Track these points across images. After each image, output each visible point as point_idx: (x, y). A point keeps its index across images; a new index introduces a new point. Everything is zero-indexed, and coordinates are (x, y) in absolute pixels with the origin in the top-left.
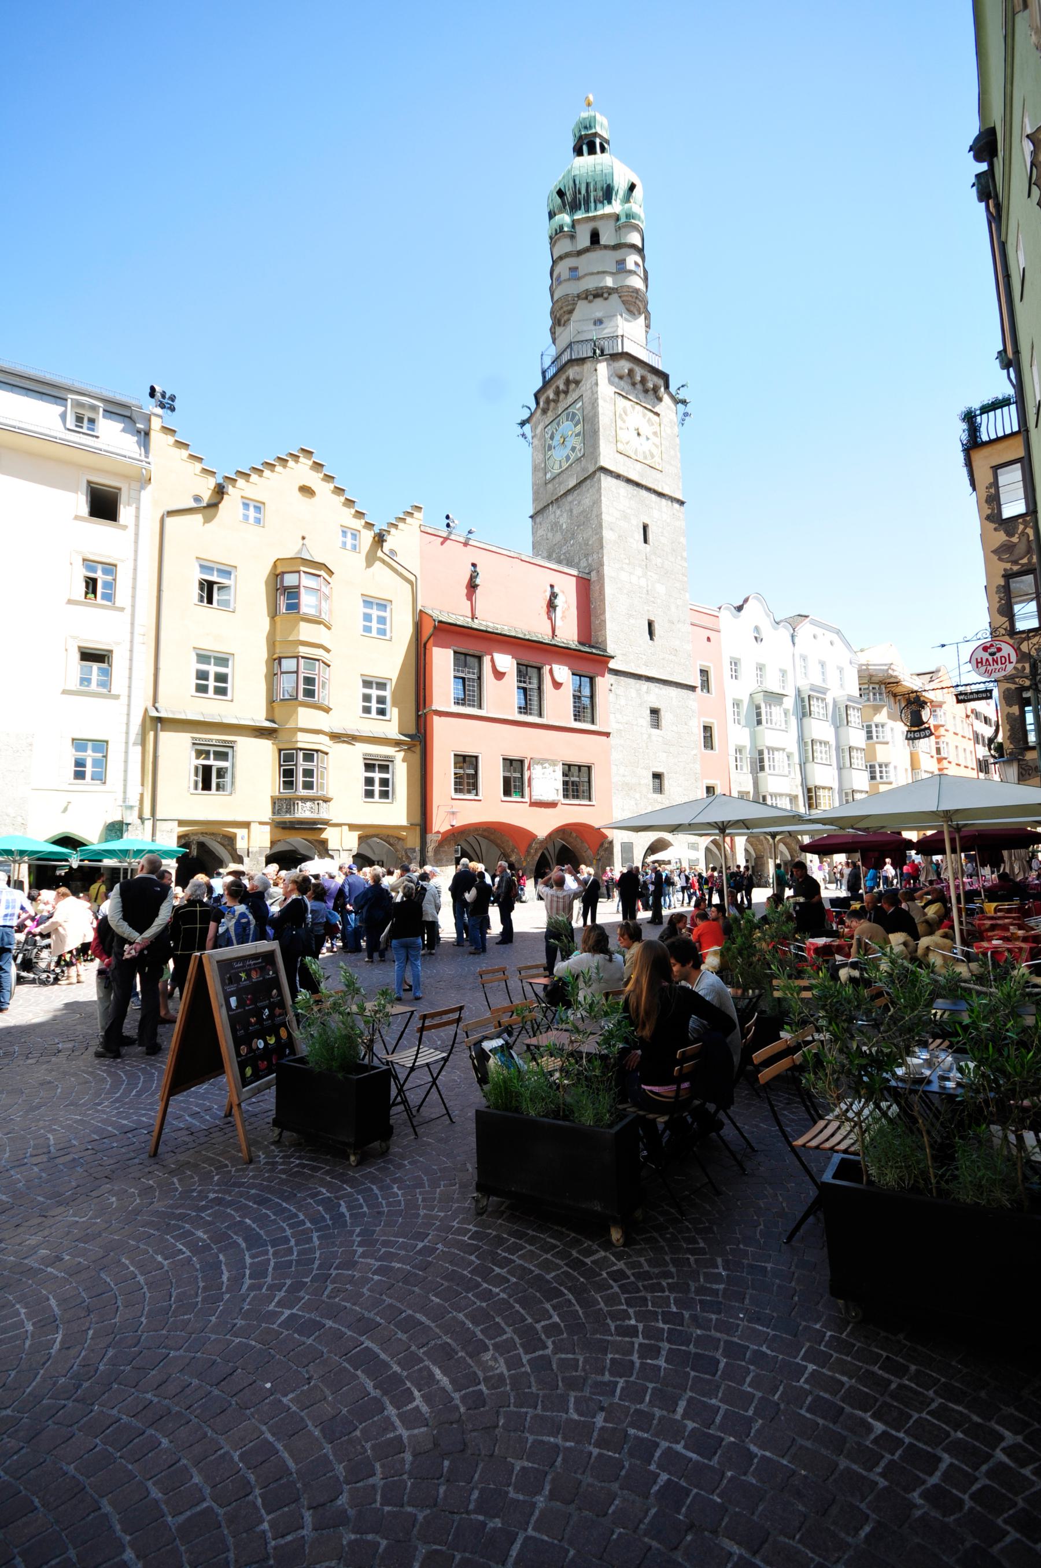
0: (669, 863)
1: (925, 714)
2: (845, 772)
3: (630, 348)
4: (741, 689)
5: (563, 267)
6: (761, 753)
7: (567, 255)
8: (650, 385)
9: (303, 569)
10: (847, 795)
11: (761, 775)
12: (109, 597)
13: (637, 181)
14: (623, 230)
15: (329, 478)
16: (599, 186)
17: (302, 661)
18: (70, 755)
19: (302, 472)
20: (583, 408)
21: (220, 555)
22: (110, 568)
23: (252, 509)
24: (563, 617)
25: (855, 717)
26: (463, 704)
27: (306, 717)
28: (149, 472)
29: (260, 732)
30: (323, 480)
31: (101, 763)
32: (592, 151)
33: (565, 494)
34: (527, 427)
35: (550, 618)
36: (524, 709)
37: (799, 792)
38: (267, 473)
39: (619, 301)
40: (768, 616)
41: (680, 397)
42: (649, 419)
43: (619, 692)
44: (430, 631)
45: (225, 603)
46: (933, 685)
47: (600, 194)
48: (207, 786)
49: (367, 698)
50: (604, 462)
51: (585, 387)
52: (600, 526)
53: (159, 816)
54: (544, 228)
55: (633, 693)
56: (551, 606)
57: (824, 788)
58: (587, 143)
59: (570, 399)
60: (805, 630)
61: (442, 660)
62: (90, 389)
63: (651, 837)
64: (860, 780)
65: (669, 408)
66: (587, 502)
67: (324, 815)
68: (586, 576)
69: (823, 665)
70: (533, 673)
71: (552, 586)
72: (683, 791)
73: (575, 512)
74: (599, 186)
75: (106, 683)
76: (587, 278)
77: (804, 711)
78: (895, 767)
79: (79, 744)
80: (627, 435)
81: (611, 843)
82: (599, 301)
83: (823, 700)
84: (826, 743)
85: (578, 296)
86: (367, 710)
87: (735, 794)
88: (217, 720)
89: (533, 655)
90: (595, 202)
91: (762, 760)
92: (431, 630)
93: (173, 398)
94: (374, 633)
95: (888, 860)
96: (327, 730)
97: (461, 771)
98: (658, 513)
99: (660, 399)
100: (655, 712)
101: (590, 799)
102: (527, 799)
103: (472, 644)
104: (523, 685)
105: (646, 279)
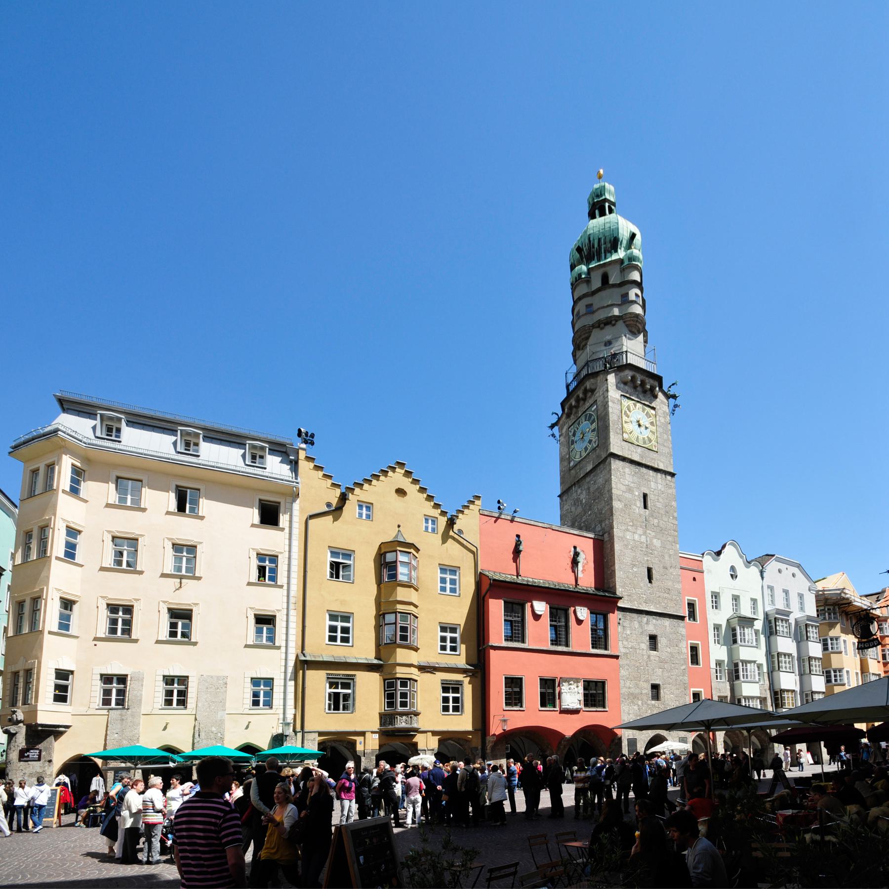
0: (664, 753)
1: (874, 628)
2: (805, 677)
3: (632, 360)
4: (721, 616)
5: (581, 306)
6: (736, 665)
7: (585, 296)
8: (648, 387)
9: (399, 548)
10: (807, 694)
11: (736, 682)
12: (273, 578)
13: (636, 231)
14: (626, 271)
15: (416, 482)
16: (608, 240)
17: (399, 615)
18: (249, 689)
19: (398, 478)
21: (342, 543)
22: (274, 559)
23: (364, 509)
24: (583, 571)
25: (813, 633)
26: (511, 640)
27: (402, 656)
28: (298, 489)
29: (370, 667)
30: (412, 483)
31: (269, 694)
32: (602, 214)
34: (556, 428)
35: (573, 571)
36: (555, 642)
37: (768, 695)
38: (374, 482)
39: (623, 325)
40: (741, 557)
41: (671, 393)
43: (625, 624)
44: (487, 588)
45: (347, 578)
46: (882, 603)
48: (337, 708)
49: (443, 639)
50: (614, 449)
51: (598, 394)
52: (611, 498)
53: (306, 729)
54: (567, 277)
56: (575, 563)
57: (788, 691)
58: (598, 207)
59: (587, 405)
60: (772, 566)
61: (496, 608)
62: (262, 436)
63: (651, 733)
64: (818, 683)
65: (662, 402)
66: (601, 481)
67: (415, 725)
68: (600, 538)
69: (786, 592)
70: (561, 614)
71: (575, 548)
72: (674, 697)
73: (591, 489)
75: (271, 638)
77: (770, 630)
78: (848, 672)
79: (255, 681)
80: (630, 427)
81: (620, 739)
82: (608, 328)
83: (787, 621)
84: (789, 655)
86: (443, 648)
87: (715, 698)
88: (343, 660)
89: (561, 600)
91: (737, 671)
92: (488, 587)
93: (313, 436)
94: (448, 592)
95: (843, 748)
96: (416, 664)
97: (510, 690)
98: (656, 484)
99: (656, 397)
100: (653, 638)
101: (604, 707)
102: (557, 709)
103: (516, 595)
104: (554, 623)
105: (644, 307)
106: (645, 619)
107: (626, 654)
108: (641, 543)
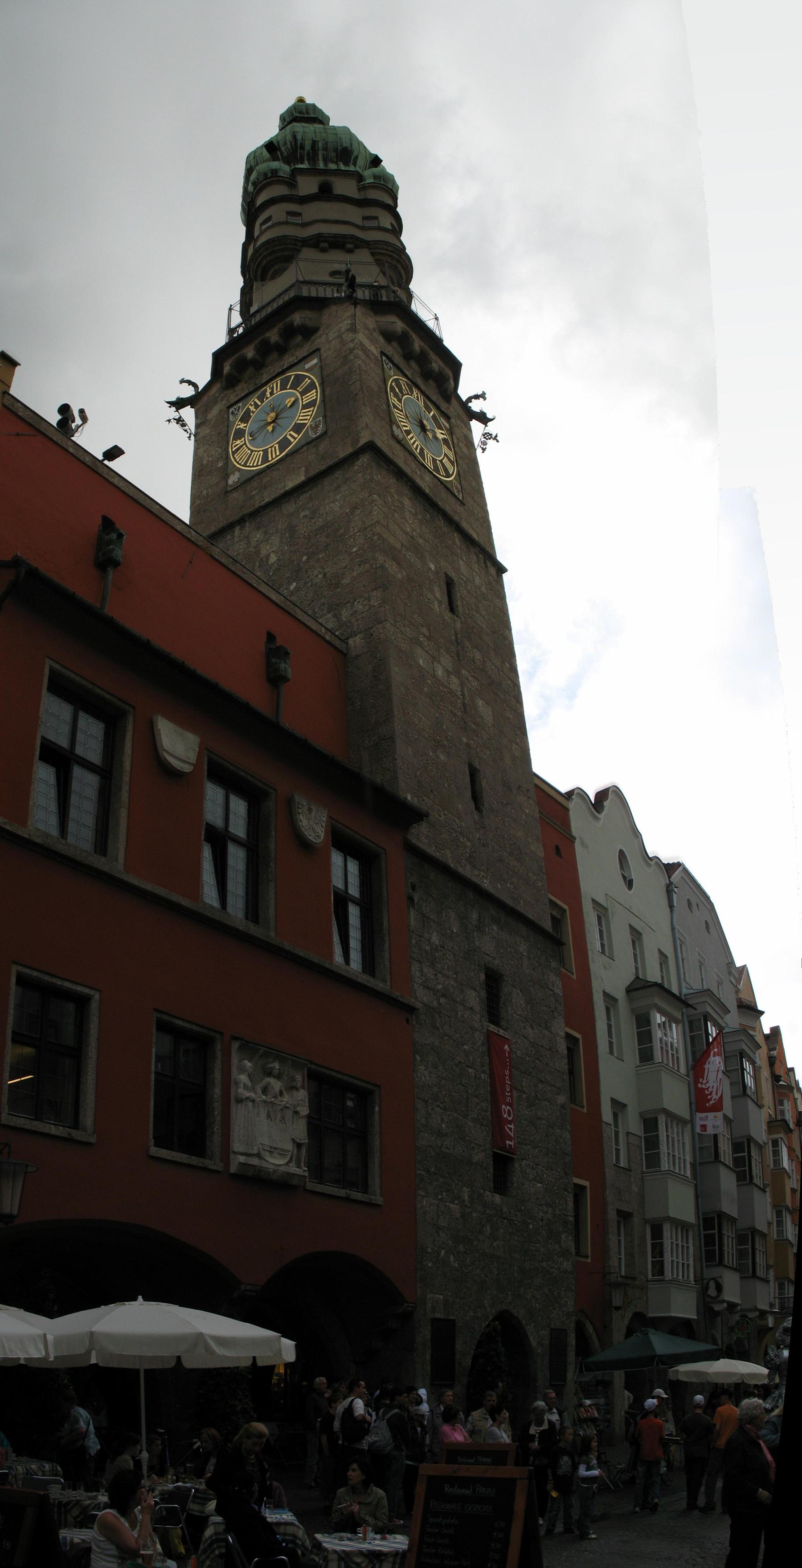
33: (277, 502)
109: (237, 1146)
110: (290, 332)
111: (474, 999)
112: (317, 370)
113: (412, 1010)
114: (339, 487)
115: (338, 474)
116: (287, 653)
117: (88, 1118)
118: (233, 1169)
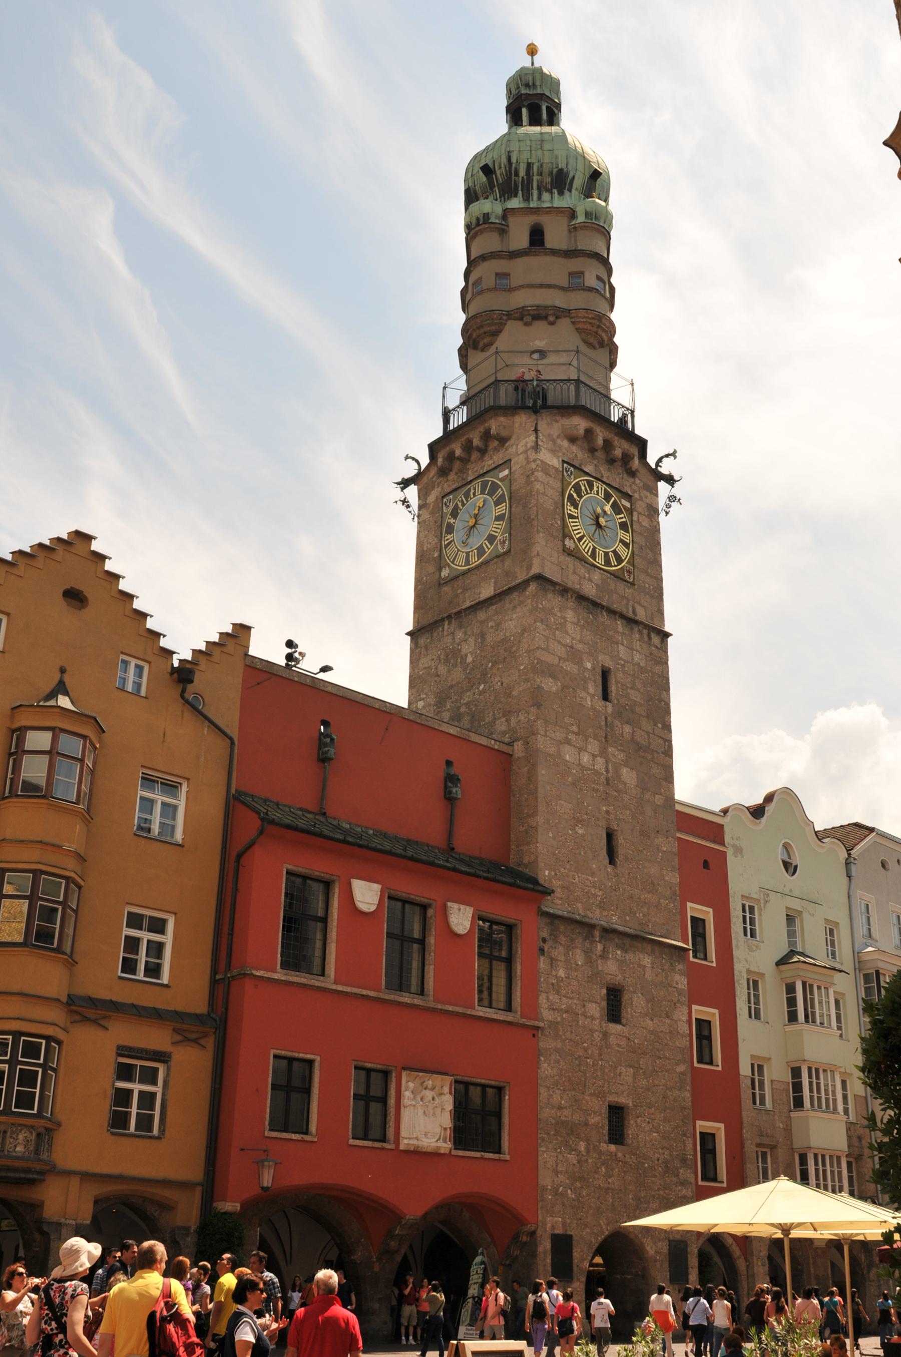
8: (618, 453)
20: (509, 479)
32: (535, 120)
42: (615, 501)
43: (554, 953)
47: (549, 179)
55: (579, 958)
68: (505, 748)
74: (546, 169)
76: (523, 291)
80: (579, 527)
82: (540, 325)
85: (509, 315)
90: (539, 188)
106: (600, 947)
107: (554, 1024)
108: (596, 773)
109: (403, 1134)
110: (487, 436)
111: (596, 1010)
112: (507, 481)
113: (538, 1028)
114: (515, 607)
115: (515, 595)
116: (458, 779)
117: (313, 1128)
118: (402, 1147)
